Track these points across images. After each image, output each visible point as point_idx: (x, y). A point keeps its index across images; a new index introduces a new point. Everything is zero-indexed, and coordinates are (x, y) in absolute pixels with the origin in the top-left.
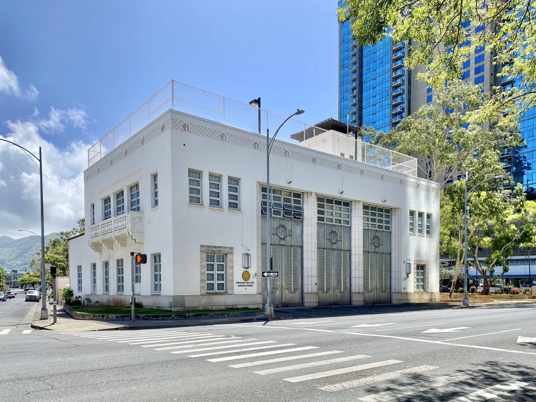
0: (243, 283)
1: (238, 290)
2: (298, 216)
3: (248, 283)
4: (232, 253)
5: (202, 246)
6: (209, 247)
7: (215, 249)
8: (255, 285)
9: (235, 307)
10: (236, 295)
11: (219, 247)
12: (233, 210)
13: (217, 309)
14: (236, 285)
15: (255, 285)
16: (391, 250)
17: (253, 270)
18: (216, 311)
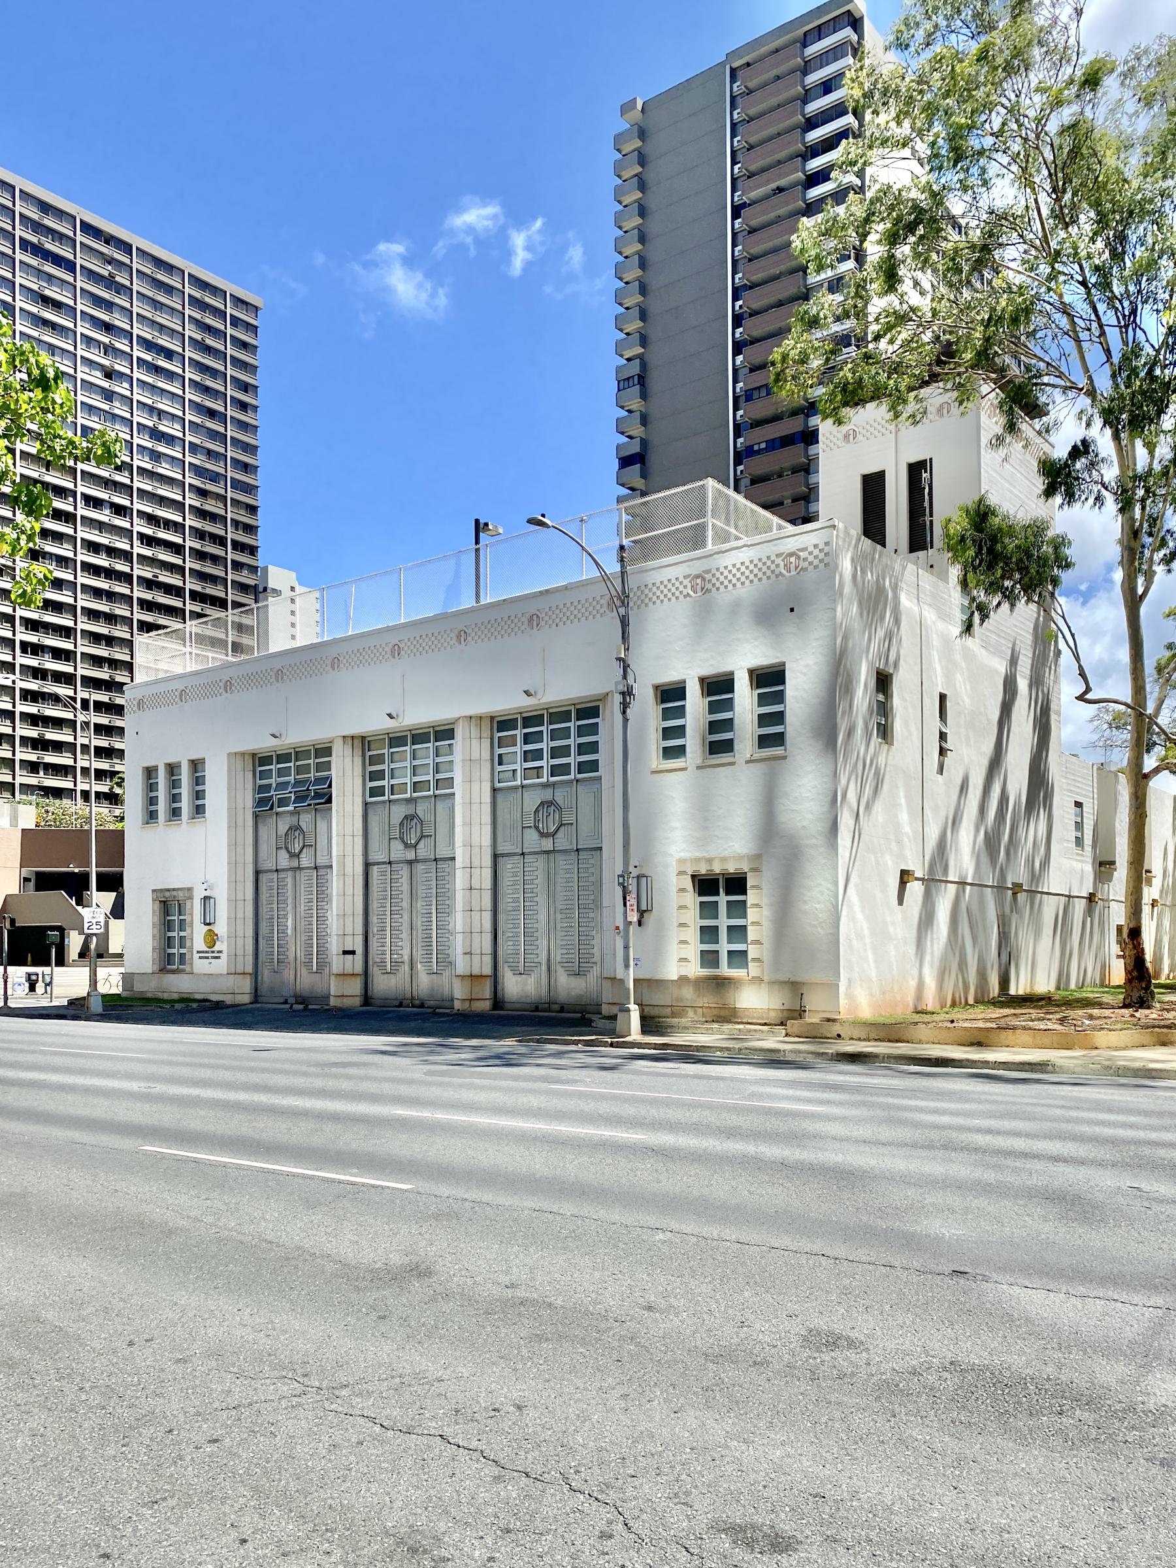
4: (191, 898)
5: (154, 891)
6: (161, 890)
7: (167, 894)
8: (224, 956)
11: (174, 890)
14: (196, 956)
15: (224, 956)
16: (600, 837)
17: (221, 928)
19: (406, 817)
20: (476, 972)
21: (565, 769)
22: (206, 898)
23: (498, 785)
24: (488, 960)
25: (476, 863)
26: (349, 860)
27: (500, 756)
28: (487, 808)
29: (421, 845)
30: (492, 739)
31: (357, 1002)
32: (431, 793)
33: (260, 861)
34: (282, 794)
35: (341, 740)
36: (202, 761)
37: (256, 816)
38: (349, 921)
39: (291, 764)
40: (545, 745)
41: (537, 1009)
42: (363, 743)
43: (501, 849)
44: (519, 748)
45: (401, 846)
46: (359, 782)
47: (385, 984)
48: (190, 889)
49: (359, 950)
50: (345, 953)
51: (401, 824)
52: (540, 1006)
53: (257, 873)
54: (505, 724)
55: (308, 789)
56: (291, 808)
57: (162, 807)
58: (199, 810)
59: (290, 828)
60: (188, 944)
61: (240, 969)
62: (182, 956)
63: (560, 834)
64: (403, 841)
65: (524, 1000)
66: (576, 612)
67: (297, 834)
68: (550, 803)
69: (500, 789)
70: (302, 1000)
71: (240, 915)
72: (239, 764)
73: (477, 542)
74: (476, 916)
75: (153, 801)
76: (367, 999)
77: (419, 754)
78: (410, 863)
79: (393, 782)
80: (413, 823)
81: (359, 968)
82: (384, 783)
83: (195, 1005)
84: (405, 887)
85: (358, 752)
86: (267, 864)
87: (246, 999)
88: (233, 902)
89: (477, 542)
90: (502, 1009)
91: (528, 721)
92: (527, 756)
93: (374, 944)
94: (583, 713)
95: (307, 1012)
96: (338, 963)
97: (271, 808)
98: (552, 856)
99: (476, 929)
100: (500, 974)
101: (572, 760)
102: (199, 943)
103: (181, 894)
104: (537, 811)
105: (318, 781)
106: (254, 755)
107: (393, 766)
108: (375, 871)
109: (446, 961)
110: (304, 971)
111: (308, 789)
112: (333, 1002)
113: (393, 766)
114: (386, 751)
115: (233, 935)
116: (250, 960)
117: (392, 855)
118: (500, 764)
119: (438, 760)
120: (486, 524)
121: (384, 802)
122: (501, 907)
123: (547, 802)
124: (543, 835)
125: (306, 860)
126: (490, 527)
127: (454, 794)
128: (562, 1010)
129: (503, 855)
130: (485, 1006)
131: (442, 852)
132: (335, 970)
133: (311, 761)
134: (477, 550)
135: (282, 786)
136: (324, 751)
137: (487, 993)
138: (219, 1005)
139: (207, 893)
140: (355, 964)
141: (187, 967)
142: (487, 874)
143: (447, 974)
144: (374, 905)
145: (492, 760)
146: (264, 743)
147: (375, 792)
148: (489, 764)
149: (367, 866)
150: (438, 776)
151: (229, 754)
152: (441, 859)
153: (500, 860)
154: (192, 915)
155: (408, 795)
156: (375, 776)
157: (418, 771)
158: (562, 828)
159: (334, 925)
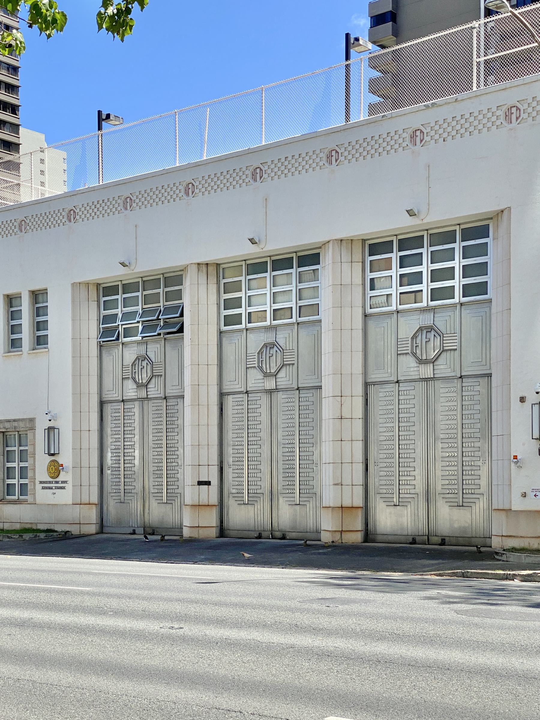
0: (50, 482)
1: (43, 496)
2: (174, 327)
3: (57, 482)
4: (33, 429)
7: (7, 425)
9: (34, 527)
10: (41, 505)
11: (14, 421)
12: (41, 350)
13: (10, 529)
14: (39, 486)
17: (66, 458)
18: (8, 531)
19: (265, 346)
20: (347, 503)
21: (449, 292)
22: (50, 429)
23: (369, 311)
24: (359, 491)
25: (347, 392)
26: (203, 390)
27: (372, 280)
28: (358, 335)
29: (282, 374)
30: (363, 262)
31: (213, 533)
32: (294, 320)
33: (105, 392)
34: (131, 324)
35: (195, 267)
36: (44, 292)
37: (100, 346)
38: (204, 452)
39: (139, 294)
40: (425, 268)
41: (414, 542)
42: (216, 269)
43: (373, 377)
44: (395, 272)
45: (260, 376)
46: (213, 309)
47: (241, 516)
48: (32, 420)
49: (215, 481)
50: (200, 483)
51: (260, 353)
52: (418, 539)
53: (102, 404)
54: (377, 247)
55: (158, 319)
56: (139, 338)
57: (26, 336)
58: (41, 341)
59: (138, 358)
60: (30, 474)
61: (85, 500)
62: (23, 487)
63: (441, 360)
64: (262, 370)
65: (399, 532)
66: (467, 125)
67: (144, 363)
68: (430, 329)
69: (371, 315)
70: (150, 531)
71: (85, 445)
72: (84, 294)
73: (347, 58)
74: (346, 446)
75: (14, 329)
76: (222, 532)
77: (279, 280)
78: (270, 392)
79: (250, 310)
80: (273, 351)
81: (214, 499)
82: (242, 311)
83: (42, 536)
84: (264, 418)
85: (213, 280)
86: (111, 394)
87: (92, 529)
88: (78, 432)
89: (347, 58)
90: (374, 541)
91: (404, 244)
92: (404, 279)
93: (229, 474)
94: (469, 233)
95: (162, 543)
96: (191, 493)
97: (118, 339)
98: (431, 383)
99: (347, 459)
100: (371, 504)
101: (457, 283)
102: (41, 472)
103: (22, 424)
104: (414, 337)
105: (167, 310)
106: (98, 285)
107: (250, 293)
108: (230, 401)
109: (309, 492)
110: (154, 504)
111: (158, 319)
112: (187, 533)
113: (250, 293)
114: (242, 278)
115: (78, 466)
116: (95, 490)
117: (250, 385)
118: (372, 288)
119: (301, 286)
120: (357, 39)
121: (240, 330)
122: (372, 437)
123: (426, 327)
124: (421, 362)
125: (154, 390)
126: (361, 42)
127: (320, 321)
128: (443, 542)
129: (374, 384)
130: (357, 538)
131: (306, 381)
132: (188, 500)
133: (161, 291)
134: (347, 66)
135: (126, 316)
136: (173, 279)
137: (359, 525)
138: (66, 536)
139: (51, 424)
140: (211, 495)
141: (29, 498)
142: (359, 402)
143: (310, 506)
144: (229, 436)
145: (364, 284)
146: (110, 272)
147: (230, 320)
148: (360, 289)
149: (222, 395)
150: (301, 303)
151: (73, 284)
152: (304, 388)
153: (372, 390)
154: (34, 445)
155: (268, 323)
156: (229, 304)
157: (278, 299)
158: (444, 355)
159: (187, 454)
